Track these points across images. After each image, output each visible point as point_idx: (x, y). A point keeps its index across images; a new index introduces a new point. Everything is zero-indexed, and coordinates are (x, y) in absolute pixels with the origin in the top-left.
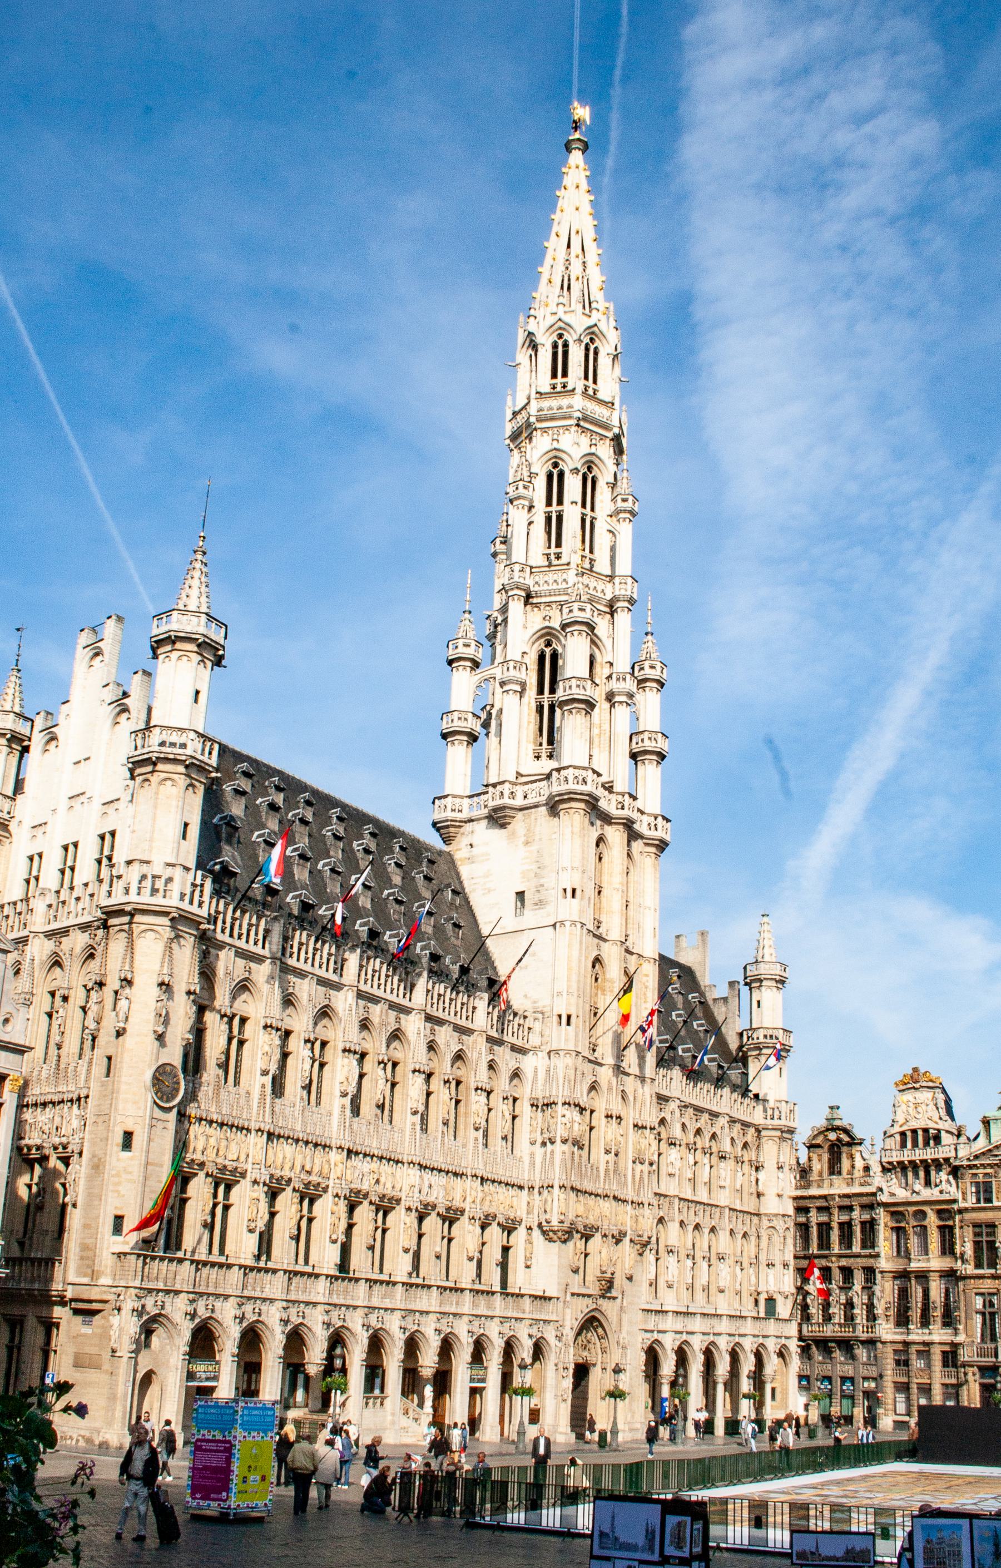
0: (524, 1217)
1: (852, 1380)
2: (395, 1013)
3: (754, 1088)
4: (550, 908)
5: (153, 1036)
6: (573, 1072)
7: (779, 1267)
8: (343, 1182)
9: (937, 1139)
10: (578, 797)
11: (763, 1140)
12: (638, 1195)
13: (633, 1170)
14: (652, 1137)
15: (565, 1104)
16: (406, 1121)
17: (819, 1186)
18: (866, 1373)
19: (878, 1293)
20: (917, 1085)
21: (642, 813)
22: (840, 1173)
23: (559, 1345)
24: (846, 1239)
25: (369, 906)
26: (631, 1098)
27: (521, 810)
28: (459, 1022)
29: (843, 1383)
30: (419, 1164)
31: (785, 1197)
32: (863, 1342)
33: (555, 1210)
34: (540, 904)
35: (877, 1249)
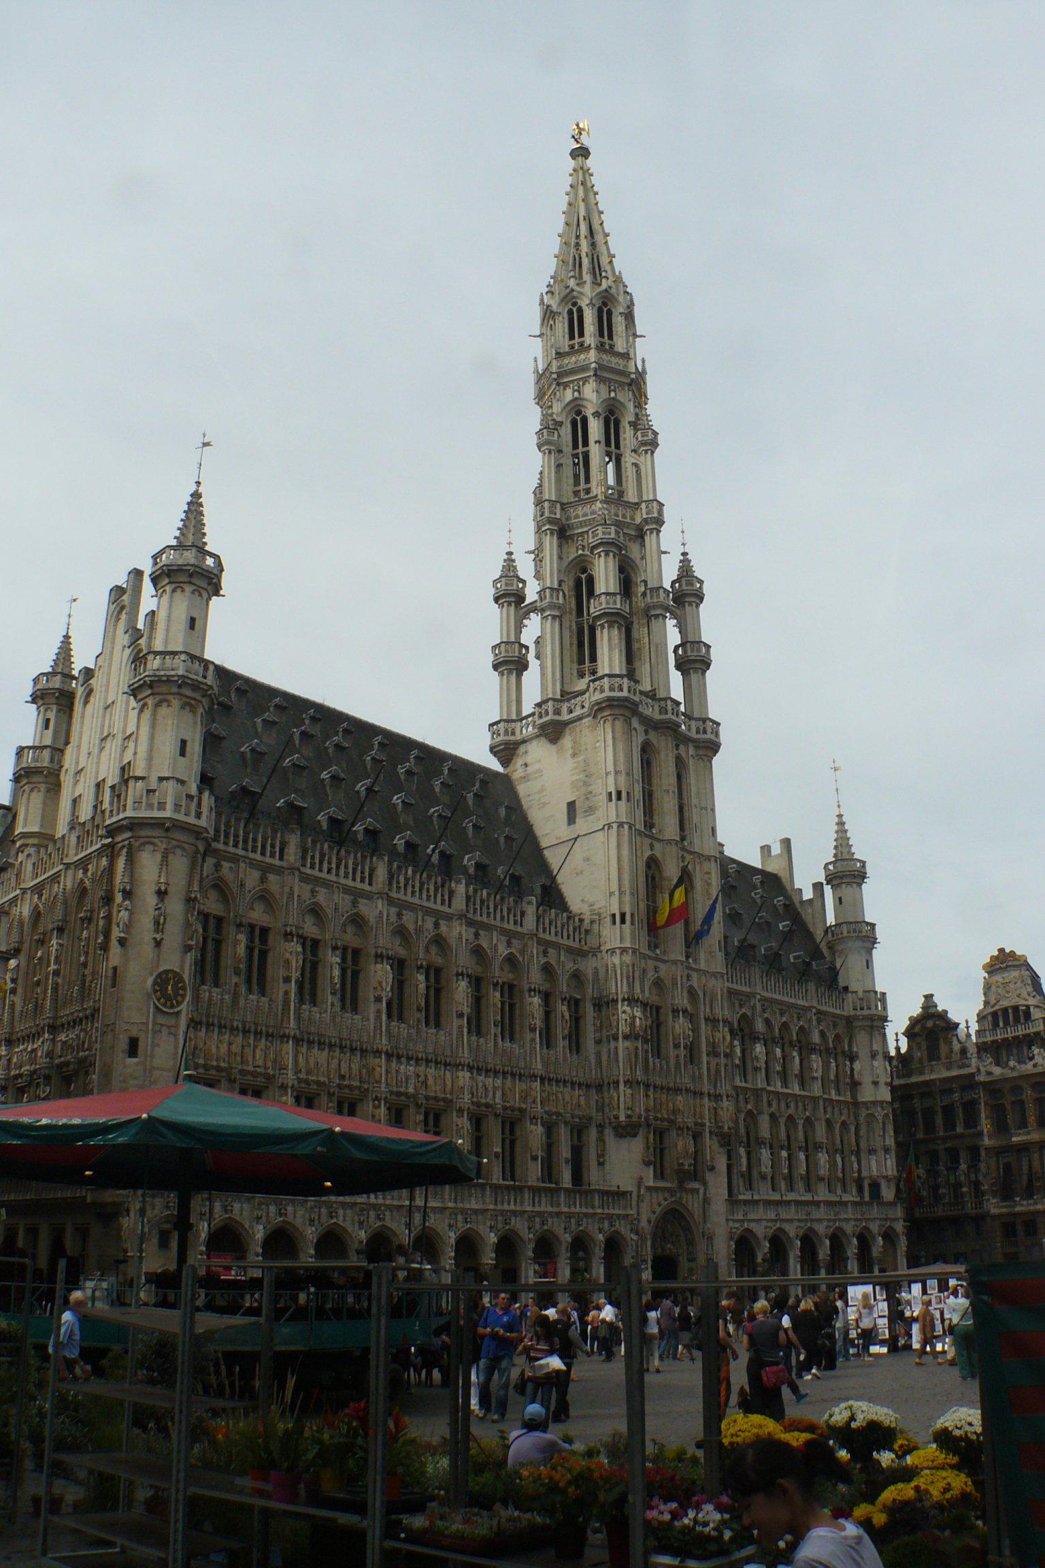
3: (842, 983)
4: (600, 813)
5: (153, 944)
6: (631, 968)
8: (383, 1085)
9: (1027, 1014)
10: (615, 703)
12: (715, 1087)
13: (708, 1063)
14: (726, 1029)
16: (455, 1025)
17: (922, 1073)
22: (939, 1059)
23: (635, 1237)
25: (411, 823)
26: (701, 995)
28: (506, 926)
30: (468, 1066)
31: (882, 1085)
33: (622, 1106)
34: (590, 810)
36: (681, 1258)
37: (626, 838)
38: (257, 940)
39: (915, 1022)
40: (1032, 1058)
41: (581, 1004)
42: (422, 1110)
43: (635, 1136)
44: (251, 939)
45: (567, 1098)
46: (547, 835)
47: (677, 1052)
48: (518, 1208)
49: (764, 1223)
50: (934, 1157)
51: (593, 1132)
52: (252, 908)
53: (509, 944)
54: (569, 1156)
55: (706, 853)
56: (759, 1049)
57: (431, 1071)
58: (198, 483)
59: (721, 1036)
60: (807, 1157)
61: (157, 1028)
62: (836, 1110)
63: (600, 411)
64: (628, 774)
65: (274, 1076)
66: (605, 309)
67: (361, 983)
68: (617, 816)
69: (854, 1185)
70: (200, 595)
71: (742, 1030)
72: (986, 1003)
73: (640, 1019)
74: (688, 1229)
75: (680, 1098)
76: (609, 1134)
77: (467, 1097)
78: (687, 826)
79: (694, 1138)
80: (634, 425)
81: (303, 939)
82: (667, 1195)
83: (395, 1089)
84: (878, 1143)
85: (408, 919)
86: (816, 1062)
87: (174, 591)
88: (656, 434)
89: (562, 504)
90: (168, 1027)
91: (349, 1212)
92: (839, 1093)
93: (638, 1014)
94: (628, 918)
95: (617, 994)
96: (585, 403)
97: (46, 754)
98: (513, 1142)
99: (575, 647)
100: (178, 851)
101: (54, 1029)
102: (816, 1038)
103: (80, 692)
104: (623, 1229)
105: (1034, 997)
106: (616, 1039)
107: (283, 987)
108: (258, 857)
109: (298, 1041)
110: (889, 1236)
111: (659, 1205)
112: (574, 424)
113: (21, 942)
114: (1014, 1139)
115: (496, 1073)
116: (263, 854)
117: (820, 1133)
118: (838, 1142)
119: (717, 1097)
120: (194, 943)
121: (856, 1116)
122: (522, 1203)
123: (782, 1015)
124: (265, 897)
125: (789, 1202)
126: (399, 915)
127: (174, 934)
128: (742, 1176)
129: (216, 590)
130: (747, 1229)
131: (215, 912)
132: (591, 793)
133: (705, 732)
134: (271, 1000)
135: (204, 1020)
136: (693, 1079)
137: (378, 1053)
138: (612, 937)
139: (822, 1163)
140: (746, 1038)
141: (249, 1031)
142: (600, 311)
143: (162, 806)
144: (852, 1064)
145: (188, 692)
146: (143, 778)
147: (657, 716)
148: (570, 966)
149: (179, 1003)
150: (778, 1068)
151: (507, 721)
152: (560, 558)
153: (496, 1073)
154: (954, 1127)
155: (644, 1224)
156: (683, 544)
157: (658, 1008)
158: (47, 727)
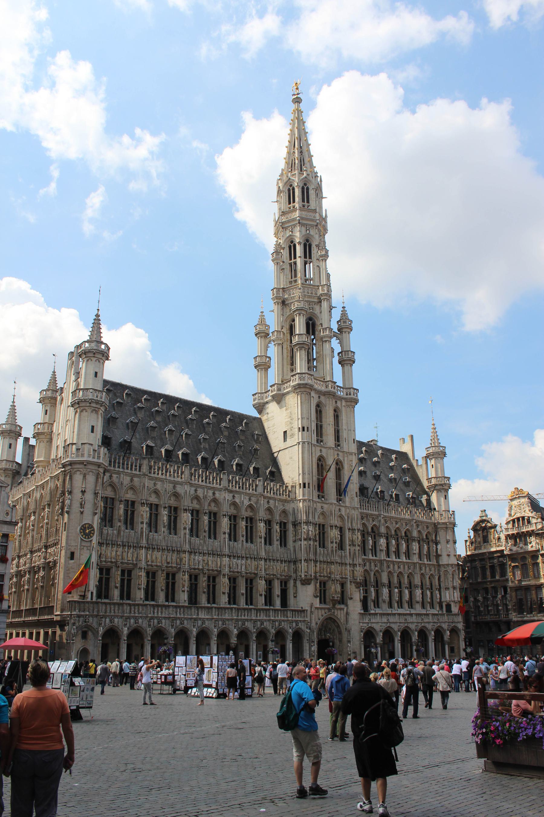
4: (296, 437)
5: (79, 513)
7: (451, 589)
8: (186, 566)
9: (529, 522)
11: (439, 530)
12: (353, 561)
14: (359, 534)
17: (480, 549)
19: (509, 598)
20: (517, 496)
23: (309, 631)
25: (207, 447)
26: (346, 518)
30: (228, 555)
34: (292, 435)
35: (507, 577)
36: (335, 641)
37: (306, 449)
38: (130, 506)
39: (477, 524)
40: (530, 543)
41: (287, 524)
42: (206, 576)
43: (309, 584)
44: (127, 505)
45: (278, 568)
47: (332, 545)
48: (249, 618)
49: (380, 624)
50: (486, 590)
51: (292, 583)
52: (127, 493)
53: (250, 500)
55: (350, 451)
56: (382, 541)
57: (211, 558)
58: (98, 310)
59: (356, 537)
60: (410, 593)
61: (82, 547)
62: (428, 569)
63: (301, 241)
64: (308, 419)
65: (136, 564)
66: (305, 187)
67: (178, 521)
68: (302, 439)
69: (438, 605)
70: (99, 362)
71: (374, 532)
72: (510, 515)
73: (312, 531)
74: (338, 627)
75: (333, 566)
76: (298, 583)
77: (227, 570)
78: (341, 439)
79: (343, 585)
80: (318, 246)
81: (151, 506)
82: (326, 611)
83: (193, 567)
84: (450, 585)
85: (200, 493)
87: (88, 361)
88: (327, 251)
89: (283, 288)
90: (87, 547)
91: (167, 621)
92: (429, 559)
93: (311, 528)
94: (307, 485)
96: (294, 237)
97: (46, 425)
98: (251, 589)
99: (289, 358)
100: (91, 473)
101: (46, 547)
103: (59, 398)
104: (302, 626)
105: (532, 512)
106: (301, 540)
107: (140, 526)
108: (129, 471)
109: (147, 548)
110: (454, 631)
111: (322, 616)
112: (290, 247)
113: (36, 508)
114: (523, 583)
115: (242, 557)
116: (131, 469)
117: (417, 580)
118: (428, 583)
119: (354, 565)
120: (97, 511)
121: (439, 571)
122: (251, 615)
123: (396, 524)
124: (132, 488)
125: (395, 614)
126: (196, 491)
127: (88, 508)
128: (374, 602)
129: (107, 359)
130: (371, 627)
131: (110, 496)
133: (350, 394)
134: (135, 532)
135: (105, 542)
136: (341, 557)
137: (184, 552)
138: (299, 494)
139: (418, 594)
140: (376, 536)
141: (125, 546)
142: (303, 188)
143: (83, 455)
144: (436, 546)
145: (94, 405)
146: (75, 444)
147: (323, 389)
148: (281, 507)
149: (91, 537)
151: (259, 393)
152: (283, 315)
153: (242, 557)
154: (495, 577)
155: (313, 624)
156: (343, 303)
157: (323, 525)
158: (46, 414)
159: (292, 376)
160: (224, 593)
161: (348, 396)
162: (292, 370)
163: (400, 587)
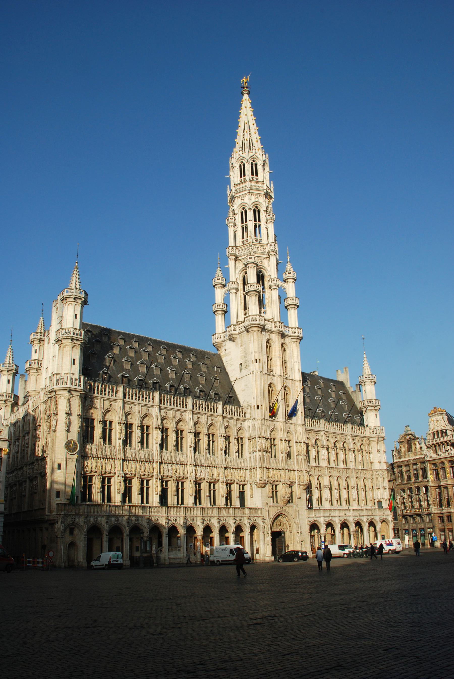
0: (249, 480)
1: (424, 529)
2: (180, 413)
4: (249, 368)
6: (260, 426)
7: (382, 490)
13: (297, 459)
14: (305, 446)
15: (258, 437)
17: (405, 457)
18: (428, 526)
21: (289, 328)
22: (412, 451)
24: (417, 476)
26: (294, 433)
27: (239, 334)
28: (210, 413)
29: (421, 531)
32: (427, 514)
33: (258, 477)
34: (247, 367)
35: (427, 478)
45: (237, 474)
46: (233, 376)
47: (282, 455)
50: (411, 490)
54: (238, 495)
57: (180, 467)
64: (259, 353)
86: (351, 456)
93: (264, 441)
94: (260, 407)
95: (256, 435)
102: (352, 446)
121: (372, 475)
132: (247, 360)
139: (354, 494)
148: (239, 426)
150: (333, 459)
159: (246, 318)
160: (191, 496)
161: (294, 334)
162: (246, 314)
163: (340, 489)
